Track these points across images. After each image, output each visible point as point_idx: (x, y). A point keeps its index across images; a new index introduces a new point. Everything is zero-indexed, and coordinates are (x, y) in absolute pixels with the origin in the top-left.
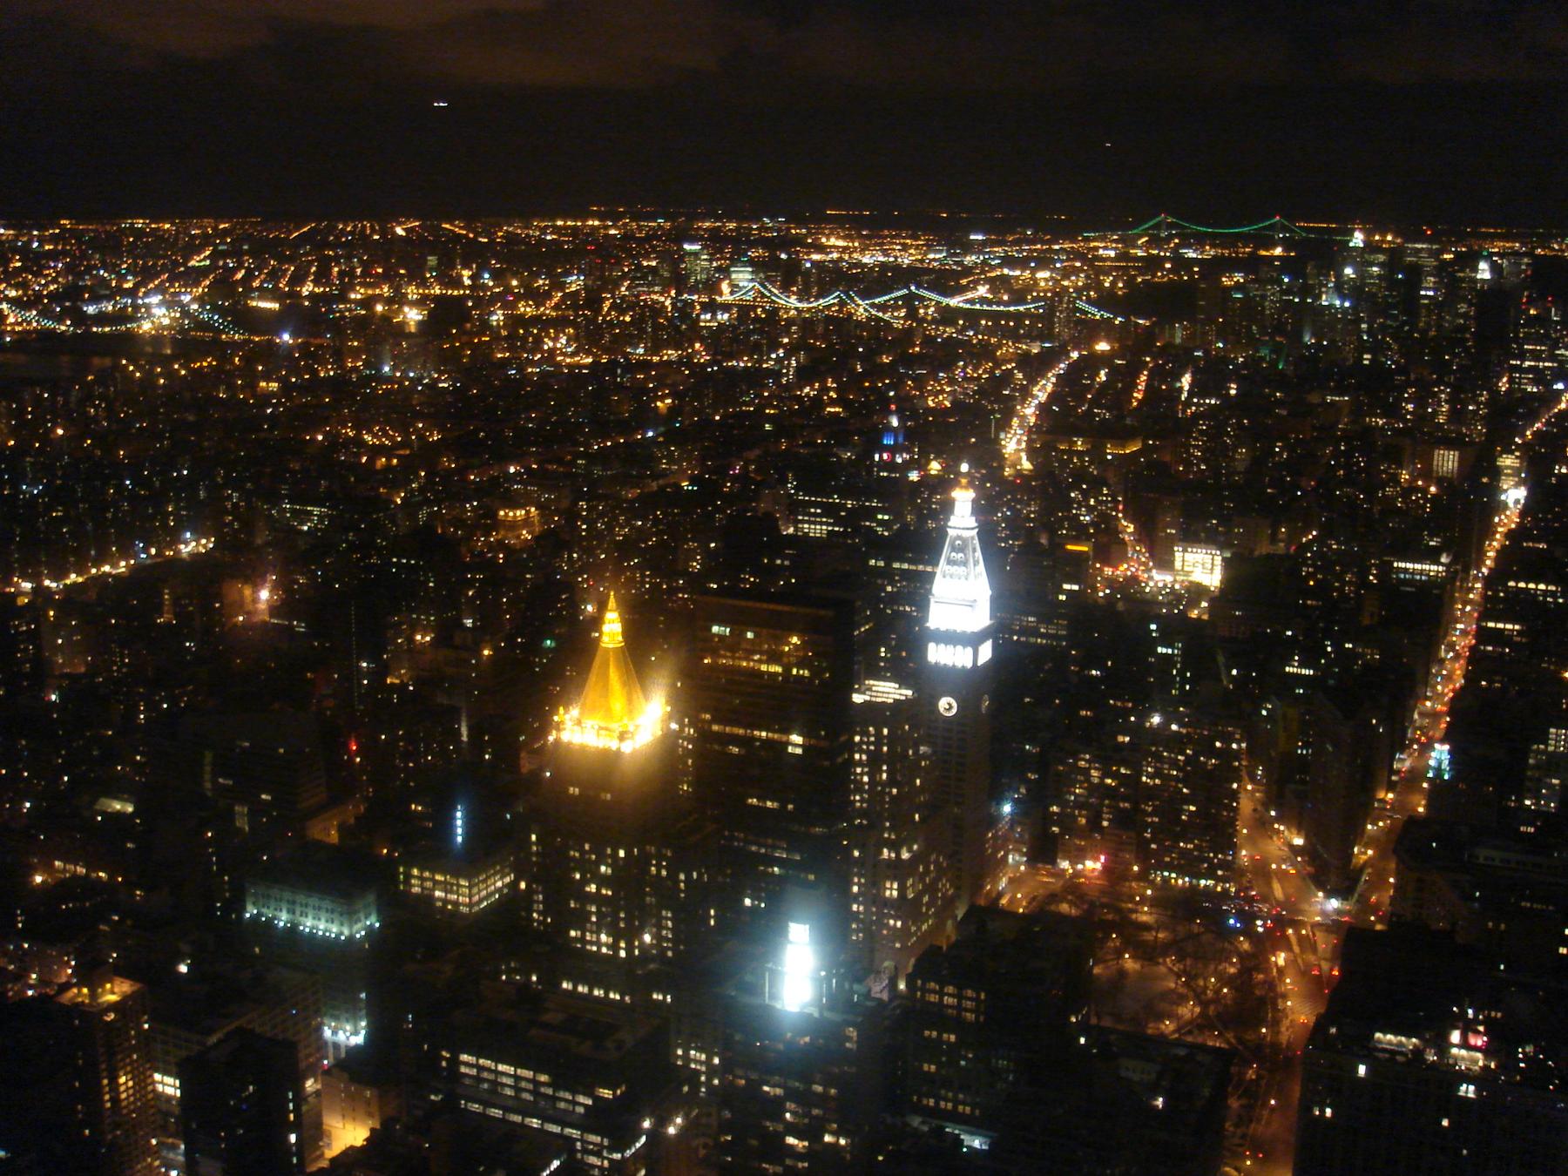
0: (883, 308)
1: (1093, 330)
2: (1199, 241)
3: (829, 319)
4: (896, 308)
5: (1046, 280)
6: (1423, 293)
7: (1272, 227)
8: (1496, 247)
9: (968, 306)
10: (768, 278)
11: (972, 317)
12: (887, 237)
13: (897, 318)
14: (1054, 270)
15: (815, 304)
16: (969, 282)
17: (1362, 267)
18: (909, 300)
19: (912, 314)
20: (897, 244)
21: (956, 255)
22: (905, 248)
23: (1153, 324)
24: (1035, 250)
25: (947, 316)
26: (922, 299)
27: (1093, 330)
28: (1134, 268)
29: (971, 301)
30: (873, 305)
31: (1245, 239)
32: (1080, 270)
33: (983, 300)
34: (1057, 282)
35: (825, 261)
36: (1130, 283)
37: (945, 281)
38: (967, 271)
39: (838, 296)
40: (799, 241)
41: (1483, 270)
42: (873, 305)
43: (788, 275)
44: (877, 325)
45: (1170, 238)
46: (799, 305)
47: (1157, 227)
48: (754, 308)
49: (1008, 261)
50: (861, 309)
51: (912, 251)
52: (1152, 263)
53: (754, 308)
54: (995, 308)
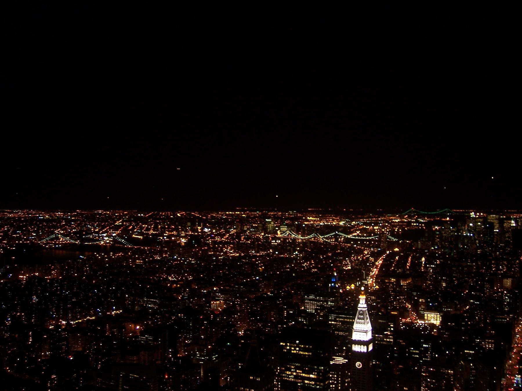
0: (326, 238)
1: (392, 245)
2: (423, 217)
3: (312, 242)
4: (331, 238)
5: (377, 229)
6: (495, 231)
7: (445, 212)
8: (514, 216)
9: (354, 238)
10: (292, 229)
11: (355, 241)
12: (327, 217)
13: (333, 241)
14: (379, 226)
15: (307, 238)
16: (353, 230)
17: (475, 223)
18: (336, 235)
19: (337, 240)
20: (331, 219)
21: (349, 222)
22: (333, 220)
23: (411, 242)
24: (374, 220)
25: (347, 240)
26: (340, 235)
27: (392, 245)
28: (404, 225)
29: (355, 236)
30: (324, 238)
31: (438, 215)
32: (388, 226)
33: (358, 235)
34: (381, 230)
35: (309, 224)
36: (403, 229)
37: (347, 230)
38: (353, 227)
39: (314, 235)
40: (301, 218)
41: (513, 223)
42: (324, 238)
43: (299, 229)
44: (326, 244)
45: (414, 216)
46: (302, 238)
47: (410, 212)
48: (288, 239)
49: (365, 224)
50: (321, 238)
51: (335, 221)
52: (409, 223)
53: (288, 239)
54: (362, 238)
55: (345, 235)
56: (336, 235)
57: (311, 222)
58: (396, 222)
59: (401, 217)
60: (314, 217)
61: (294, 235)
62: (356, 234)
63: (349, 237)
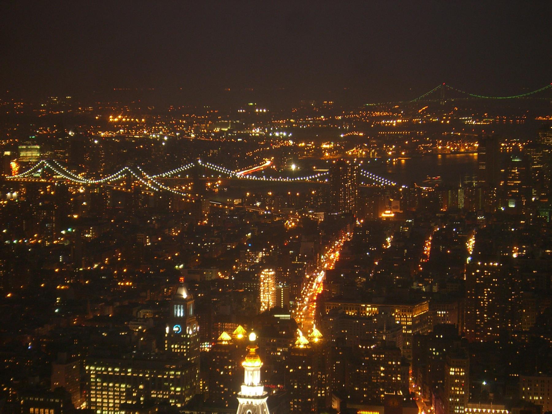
0: (166, 182)
3: (117, 194)
5: (330, 150)
10: (54, 156)
14: (336, 139)
16: (254, 155)
18: (196, 172)
19: (199, 186)
26: (209, 172)
29: (257, 174)
30: (161, 180)
33: (268, 171)
35: (112, 137)
42: (161, 180)
53: (44, 185)
54: (280, 179)
55: (223, 170)
56: (196, 172)
57: (119, 129)
58: (391, 128)
59: (410, 113)
60: (130, 115)
61: (62, 176)
62: (261, 167)
63: (240, 174)
